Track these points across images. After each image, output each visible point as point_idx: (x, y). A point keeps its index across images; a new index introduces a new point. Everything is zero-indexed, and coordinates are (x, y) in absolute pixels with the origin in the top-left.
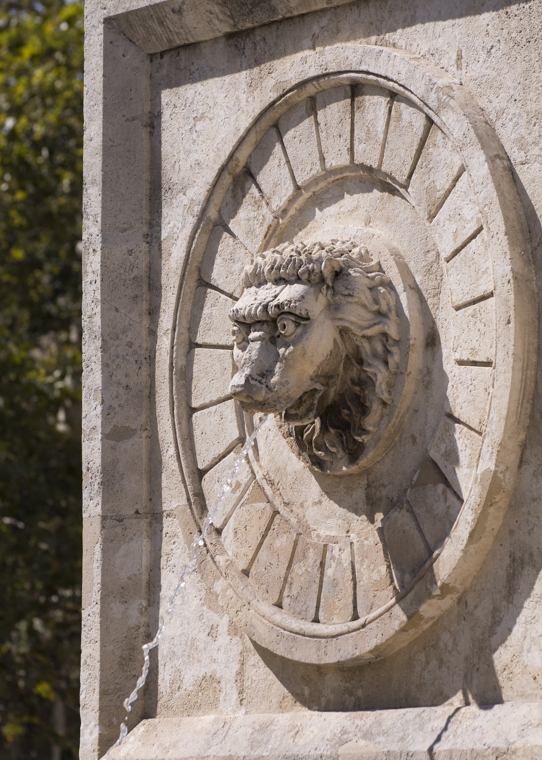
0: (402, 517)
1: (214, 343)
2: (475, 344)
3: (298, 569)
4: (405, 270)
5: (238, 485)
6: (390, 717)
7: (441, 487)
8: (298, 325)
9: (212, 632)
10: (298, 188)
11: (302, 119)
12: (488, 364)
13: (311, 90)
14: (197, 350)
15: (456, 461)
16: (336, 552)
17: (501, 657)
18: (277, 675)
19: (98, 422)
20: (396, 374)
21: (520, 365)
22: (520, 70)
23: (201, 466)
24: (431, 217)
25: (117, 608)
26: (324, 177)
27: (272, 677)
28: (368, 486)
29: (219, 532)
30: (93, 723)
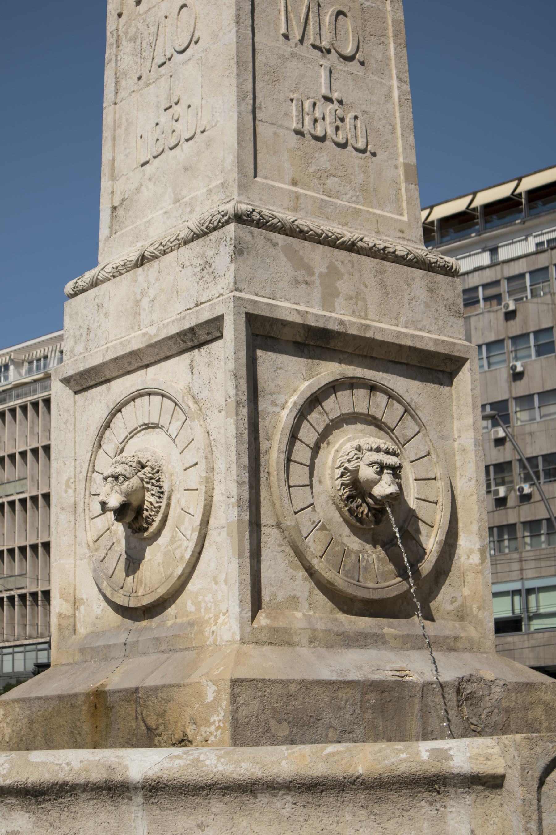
1: (301, 462)
5: (314, 522)
9: (293, 578)
11: (346, 389)
13: (354, 381)
14: (291, 463)
15: (420, 533)
18: (330, 599)
27: (327, 600)
28: (373, 534)
30: (247, 609)
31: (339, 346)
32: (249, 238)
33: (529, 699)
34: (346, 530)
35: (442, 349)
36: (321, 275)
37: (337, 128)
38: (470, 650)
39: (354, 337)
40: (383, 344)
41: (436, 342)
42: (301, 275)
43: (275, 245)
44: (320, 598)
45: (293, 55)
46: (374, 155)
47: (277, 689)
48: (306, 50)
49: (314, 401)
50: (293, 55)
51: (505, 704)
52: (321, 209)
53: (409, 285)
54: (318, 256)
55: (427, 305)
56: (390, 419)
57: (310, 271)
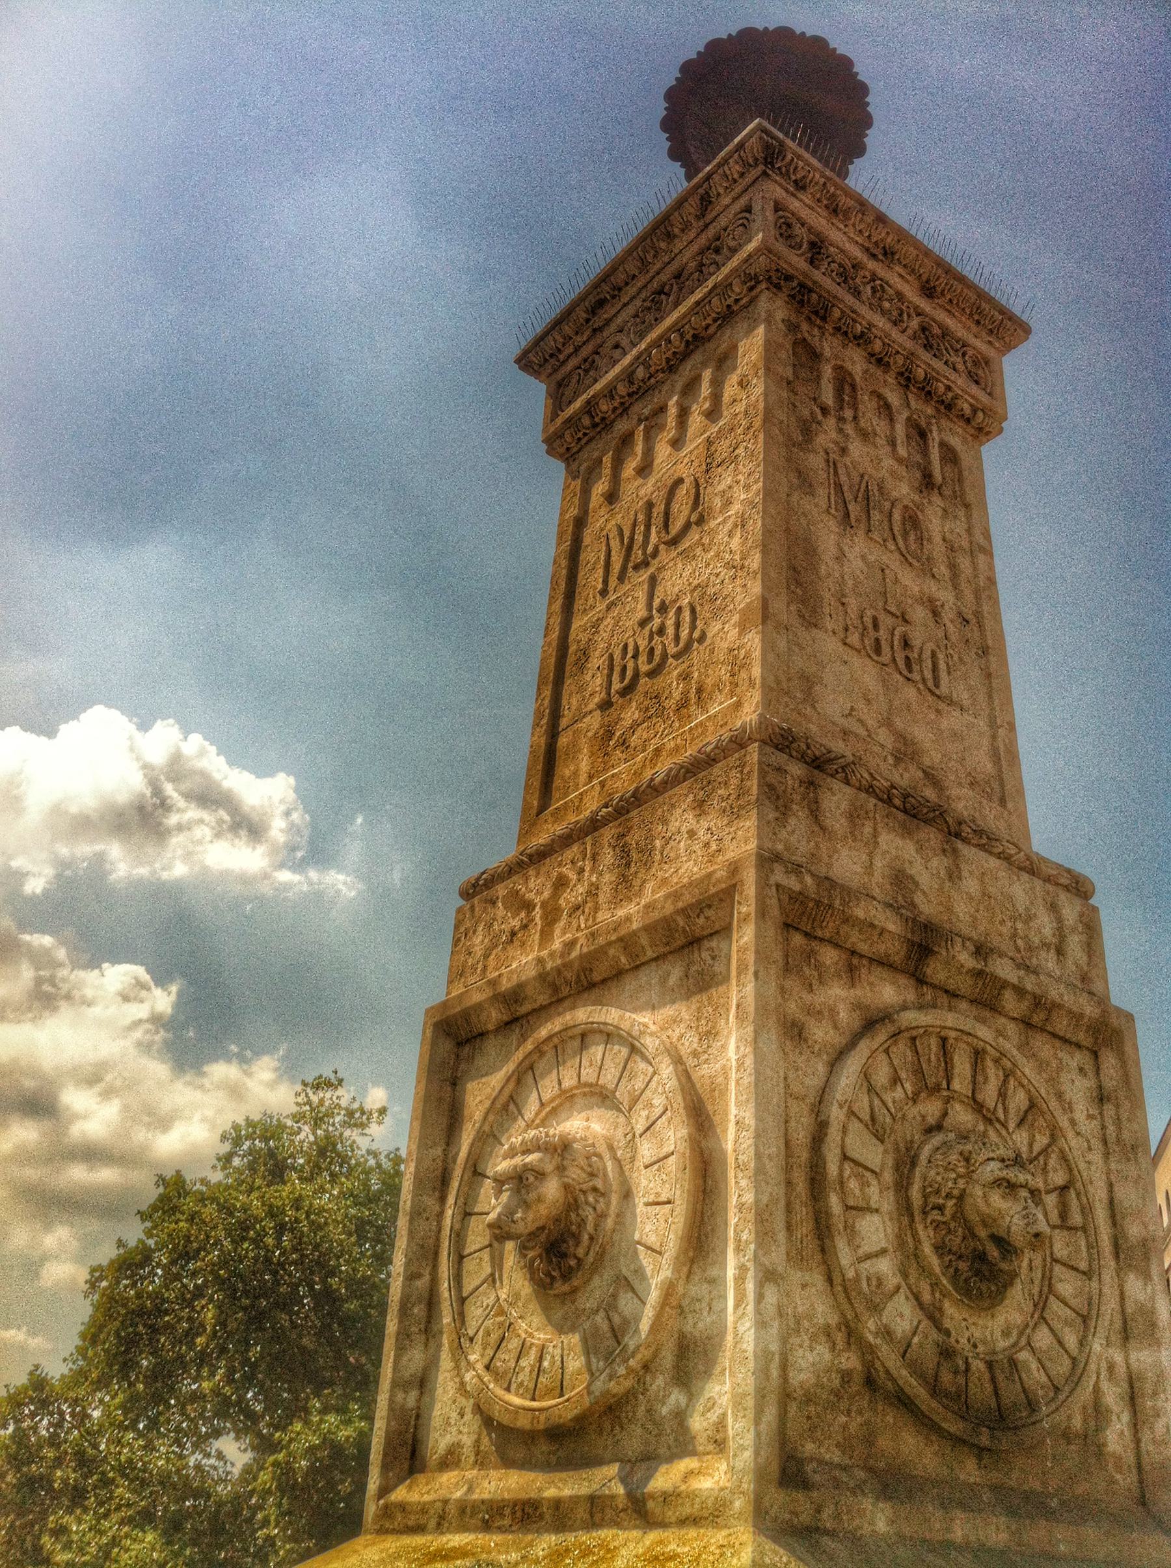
2: (659, 1190)
3: (524, 1363)
4: (611, 1148)
7: (630, 1295)
8: (536, 1178)
10: (542, 1105)
12: (669, 1202)
16: (551, 1349)
19: (402, 1270)
20: (601, 1216)
21: (691, 1199)
22: (694, 1007)
23: (465, 1295)
24: (631, 1109)
25: (400, 1396)
26: (559, 1096)
29: (471, 1340)
36: (544, 905)
57: (529, 906)
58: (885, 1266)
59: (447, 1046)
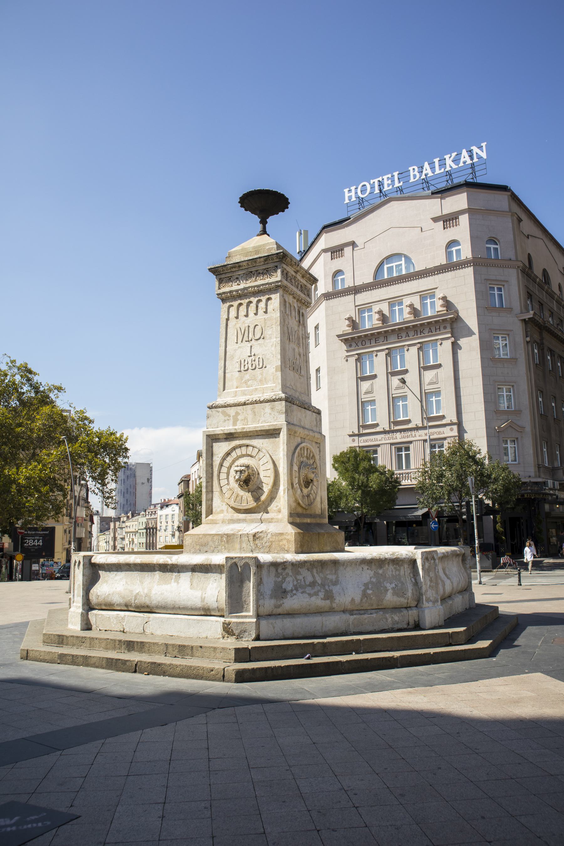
0: (255, 493)
6: (253, 515)
9: (222, 505)
17: (269, 509)
31: (237, 436)
32: (211, 413)
33: (280, 538)
34: (240, 489)
35: (271, 428)
36: (233, 416)
37: (252, 365)
38: (278, 522)
39: (240, 432)
40: (250, 432)
41: (269, 426)
42: (226, 418)
43: (219, 412)
44: (230, 510)
45: (239, 347)
46: (266, 367)
47: (196, 537)
48: (245, 343)
49: (228, 454)
50: (239, 347)
51: (271, 540)
52: (244, 393)
53: (263, 409)
54: (232, 411)
55: (270, 414)
56: (254, 454)
57: (229, 416)
58: (298, 485)
59: (210, 439)
